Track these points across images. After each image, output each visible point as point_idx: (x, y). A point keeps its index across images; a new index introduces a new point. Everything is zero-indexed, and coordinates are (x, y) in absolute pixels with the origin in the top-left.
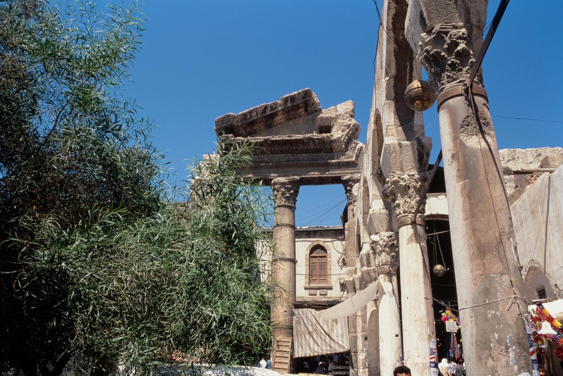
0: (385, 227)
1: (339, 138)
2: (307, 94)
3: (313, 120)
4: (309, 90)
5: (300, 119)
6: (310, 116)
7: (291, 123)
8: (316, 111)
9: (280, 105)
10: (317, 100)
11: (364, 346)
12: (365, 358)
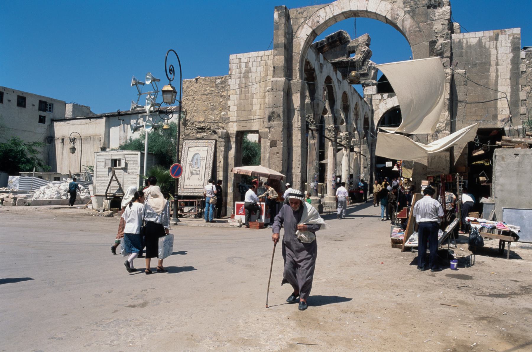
0: (345, 130)
1: (358, 60)
2: (340, 34)
3: (345, 48)
4: (341, 31)
5: (338, 48)
6: (343, 45)
7: (333, 50)
8: (347, 42)
9: (325, 42)
10: (347, 35)
11: (364, 171)
12: (364, 176)
